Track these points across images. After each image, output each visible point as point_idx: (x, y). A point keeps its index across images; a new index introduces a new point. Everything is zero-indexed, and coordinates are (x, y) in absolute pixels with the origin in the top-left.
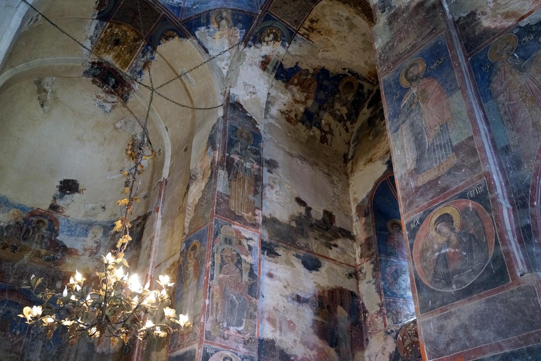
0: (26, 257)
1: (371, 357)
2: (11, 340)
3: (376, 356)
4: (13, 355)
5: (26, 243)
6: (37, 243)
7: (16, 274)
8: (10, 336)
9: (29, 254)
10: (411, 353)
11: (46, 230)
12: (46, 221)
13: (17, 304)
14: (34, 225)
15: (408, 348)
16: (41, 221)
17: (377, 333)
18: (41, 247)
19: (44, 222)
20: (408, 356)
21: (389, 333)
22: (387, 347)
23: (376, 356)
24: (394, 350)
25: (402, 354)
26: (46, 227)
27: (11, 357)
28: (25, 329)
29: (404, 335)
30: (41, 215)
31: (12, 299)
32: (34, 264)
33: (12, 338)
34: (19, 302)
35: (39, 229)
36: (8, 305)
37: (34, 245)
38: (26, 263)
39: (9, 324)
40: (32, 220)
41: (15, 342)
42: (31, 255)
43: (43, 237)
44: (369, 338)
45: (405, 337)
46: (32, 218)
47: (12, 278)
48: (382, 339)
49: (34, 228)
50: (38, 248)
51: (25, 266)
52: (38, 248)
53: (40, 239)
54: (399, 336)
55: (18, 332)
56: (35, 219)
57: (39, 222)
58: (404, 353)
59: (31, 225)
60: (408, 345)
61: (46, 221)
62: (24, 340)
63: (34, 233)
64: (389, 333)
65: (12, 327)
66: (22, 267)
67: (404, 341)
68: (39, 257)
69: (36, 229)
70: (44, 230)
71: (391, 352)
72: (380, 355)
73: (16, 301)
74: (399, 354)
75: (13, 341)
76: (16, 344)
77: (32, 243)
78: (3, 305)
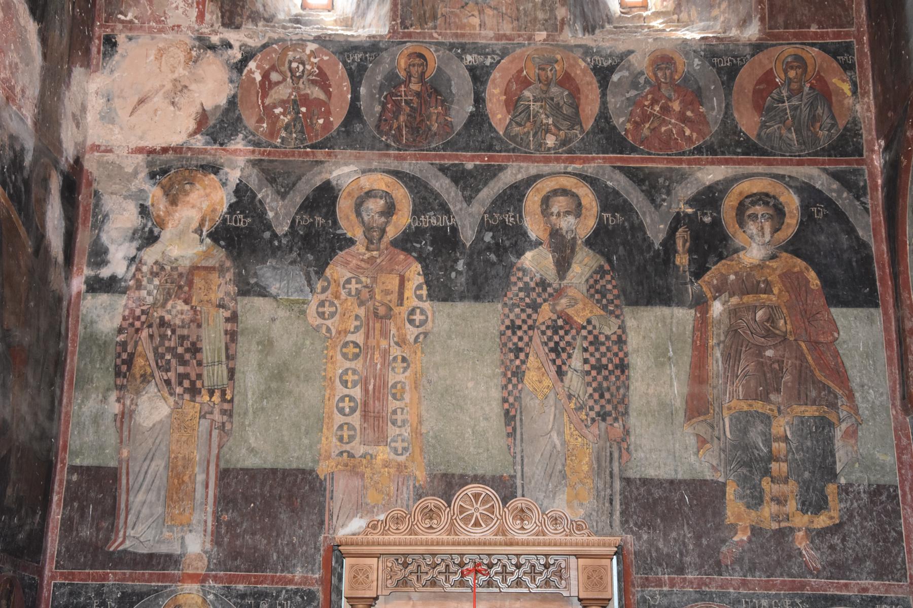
1: (117, 103)
3: (141, 101)
10: (287, 127)
15: (278, 111)
17: (161, 31)
20: (272, 133)
21: (213, 48)
22: (193, 87)
23: (141, 101)
24: (223, 101)
25: (250, 121)
29: (273, 68)
44: (121, 39)
45: (275, 77)
48: (182, 56)
54: (252, 65)
58: (260, 121)
60: (283, 103)
64: (213, 48)
67: (267, 85)
71: (208, 106)
72: (158, 100)
74: (239, 119)
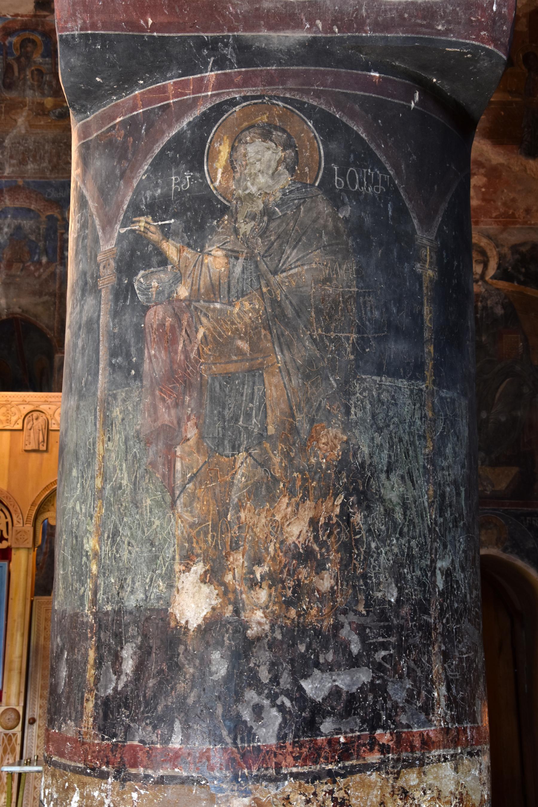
0: (21, 121)
2: (37, 274)
4: (46, 298)
5: (13, 95)
6: (32, 87)
7: (11, 157)
8: (32, 268)
9: (25, 114)
11: (43, 56)
12: (38, 38)
13: (29, 210)
14: (16, 54)
16: (29, 40)
18: (43, 94)
19: (33, 42)
26: (41, 49)
27: (44, 303)
28: (55, 252)
30: (25, 27)
31: (18, 204)
32: (39, 131)
33: (37, 270)
34: (32, 207)
35: (28, 58)
36: (14, 217)
37: (29, 92)
38: (23, 132)
39: (26, 249)
40: (10, 43)
41: (44, 277)
42: (28, 116)
43: (40, 72)
46: (10, 39)
47: (7, 167)
49: (18, 59)
50: (38, 98)
51: (24, 138)
52: (38, 98)
53: (36, 78)
55: (44, 260)
56: (14, 39)
57: (24, 43)
59: (12, 54)
61: (38, 38)
62: (58, 271)
63: (22, 69)
65: (32, 253)
66: (19, 143)
68: (44, 114)
69: (23, 59)
70: (38, 58)
73: (25, 205)
75: (40, 276)
76: (46, 280)
77: (24, 91)
78: (6, 217)
